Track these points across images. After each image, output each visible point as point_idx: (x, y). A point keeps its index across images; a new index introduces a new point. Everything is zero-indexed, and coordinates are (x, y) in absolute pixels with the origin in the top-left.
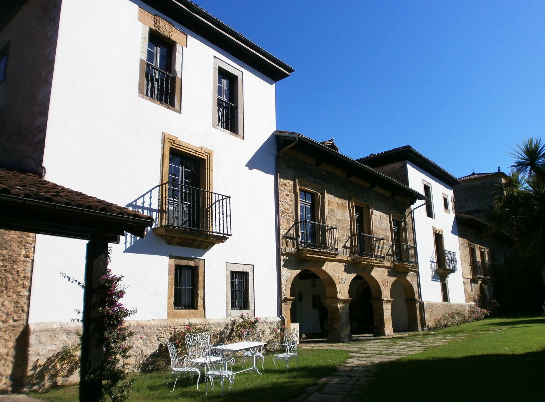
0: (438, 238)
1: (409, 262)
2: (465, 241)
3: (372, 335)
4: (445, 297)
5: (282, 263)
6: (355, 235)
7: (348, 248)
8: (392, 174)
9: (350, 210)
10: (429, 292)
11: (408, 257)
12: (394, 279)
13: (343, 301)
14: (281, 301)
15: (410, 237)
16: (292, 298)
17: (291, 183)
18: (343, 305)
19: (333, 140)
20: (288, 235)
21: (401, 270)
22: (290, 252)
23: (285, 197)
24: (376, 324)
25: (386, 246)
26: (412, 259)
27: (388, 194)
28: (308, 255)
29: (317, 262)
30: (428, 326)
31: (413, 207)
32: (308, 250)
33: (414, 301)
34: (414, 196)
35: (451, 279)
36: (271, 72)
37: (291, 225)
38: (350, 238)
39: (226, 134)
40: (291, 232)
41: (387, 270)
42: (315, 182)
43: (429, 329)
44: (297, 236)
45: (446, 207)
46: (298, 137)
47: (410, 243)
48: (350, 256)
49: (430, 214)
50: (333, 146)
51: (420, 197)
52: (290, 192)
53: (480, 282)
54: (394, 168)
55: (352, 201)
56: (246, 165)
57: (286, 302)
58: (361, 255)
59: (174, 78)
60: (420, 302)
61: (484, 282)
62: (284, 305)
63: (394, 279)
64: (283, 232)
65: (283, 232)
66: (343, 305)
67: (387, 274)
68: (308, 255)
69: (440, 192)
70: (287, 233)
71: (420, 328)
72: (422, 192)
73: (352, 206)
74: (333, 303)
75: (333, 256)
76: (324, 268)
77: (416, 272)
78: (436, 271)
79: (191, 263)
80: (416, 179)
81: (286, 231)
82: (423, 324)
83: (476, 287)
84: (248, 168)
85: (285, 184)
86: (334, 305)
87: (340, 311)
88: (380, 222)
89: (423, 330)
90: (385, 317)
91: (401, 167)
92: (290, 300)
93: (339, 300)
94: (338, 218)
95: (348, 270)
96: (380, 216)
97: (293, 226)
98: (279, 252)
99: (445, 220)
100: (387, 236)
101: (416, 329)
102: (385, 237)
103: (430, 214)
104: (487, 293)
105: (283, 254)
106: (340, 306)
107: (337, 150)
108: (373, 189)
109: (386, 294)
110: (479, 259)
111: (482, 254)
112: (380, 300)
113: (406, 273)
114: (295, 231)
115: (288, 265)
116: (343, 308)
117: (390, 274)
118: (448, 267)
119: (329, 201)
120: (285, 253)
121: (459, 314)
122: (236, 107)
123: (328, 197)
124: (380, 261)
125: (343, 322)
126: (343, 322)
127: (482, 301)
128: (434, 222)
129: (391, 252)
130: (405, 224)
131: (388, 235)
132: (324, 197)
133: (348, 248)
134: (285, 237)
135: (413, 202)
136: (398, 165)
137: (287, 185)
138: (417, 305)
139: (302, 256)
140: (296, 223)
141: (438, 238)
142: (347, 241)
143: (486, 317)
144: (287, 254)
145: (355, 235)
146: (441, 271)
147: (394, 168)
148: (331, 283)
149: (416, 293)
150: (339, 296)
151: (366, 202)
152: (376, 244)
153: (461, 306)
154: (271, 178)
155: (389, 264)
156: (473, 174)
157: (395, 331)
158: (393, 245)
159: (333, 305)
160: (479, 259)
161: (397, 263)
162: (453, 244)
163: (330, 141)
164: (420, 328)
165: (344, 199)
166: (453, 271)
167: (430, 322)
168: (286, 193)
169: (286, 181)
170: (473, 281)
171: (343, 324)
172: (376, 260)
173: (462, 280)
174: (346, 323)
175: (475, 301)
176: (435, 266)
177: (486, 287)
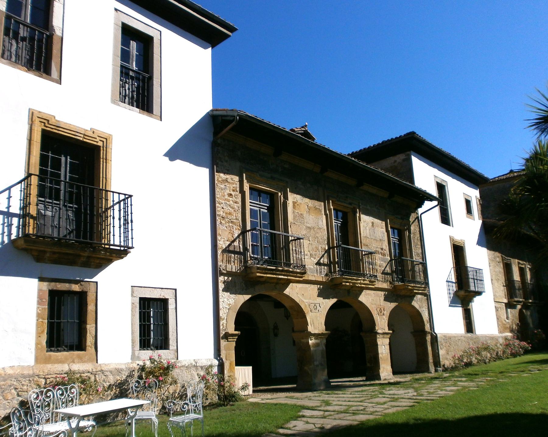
0: (458, 251)
1: (415, 282)
2: (497, 254)
3: (364, 378)
4: (469, 327)
5: (221, 286)
6: (333, 248)
7: (324, 265)
8: (392, 170)
9: (326, 214)
10: (446, 321)
11: (414, 276)
12: (393, 305)
13: (317, 336)
14: (219, 337)
15: (416, 250)
16: (237, 332)
17: (236, 178)
18: (317, 341)
19: (306, 126)
20: (231, 248)
21: (403, 293)
22: (234, 270)
23: (226, 197)
24: (368, 365)
25: (381, 262)
26: (420, 278)
27: (383, 194)
28: (258, 274)
29: (277, 283)
30: (444, 366)
31: (420, 211)
32: (258, 268)
33: (424, 333)
34: (422, 197)
35: (477, 304)
36: (204, 31)
37: (236, 235)
38: (327, 251)
39: (134, 115)
40: (236, 244)
41: (383, 293)
42: (273, 178)
43: (445, 370)
44: (245, 249)
45: (469, 210)
46: (238, 115)
47: (417, 258)
48: (326, 275)
49: (445, 219)
50: (306, 134)
51: (430, 198)
52: (234, 191)
53: (519, 307)
54: (395, 161)
55: (329, 203)
56: (166, 155)
57: (227, 339)
58: (343, 273)
59: (50, 38)
60: (432, 335)
61: (525, 306)
62: (223, 343)
63: (393, 305)
64: (222, 244)
65: (222, 244)
66: (317, 341)
67: (382, 298)
68: (258, 274)
69: (459, 191)
70: (229, 245)
71: (432, 368)
72: (433, 191)
73: (330, 210)
74: (303, 339)
75: (300, 275)
76: (288, 291)
77: (425, 295)
78: (456, 294)
79: (76, 288)
80: (425, 175)
81: (228, 243)
82: (437, 363)
83: (514, 313)
84: (167, 158)
85: (226, 181)
86: (304, 341)
87: (312, 349)
88: (372, 231)
89: (436, 371)
90: (380, 356)
91: (404, 160)
92: (233, 335)
93: (310, 334)
94: (308, 225)
95: (323, 294)
96: (373, 223)
97: (238, 236)
98: (216, 272)
99: (468, 228)
100: (382, 249)
101: (427, 370)
102: (380, 251)
103: (445, 219)
104: (530, 321)
105: (222, 274)
106: (312, 342)
107: (314, 139)
108: (361, 188)
109: (382, 324)
110: (516, 277)
111: (522, 271)
112: (373, 332)
113: (412, 296)
114: (241, 243)
115: (229, 288)
116: (316, 345)
117: (387, 299)
118: (472, 288)
119: (294, 203)
120: (225, 272)
121: (487, 349)
122: (151, 78)
123: (292, 198)
124: (370, 281)
125: (316, 363)
126: (316, 363)
127: (522, 331)
128: (451, 230)
129: (388, 270)
130: (410, 232)
131: (384, 247)
132: (286, 198)
133: (324, 265)
134: (226, 251)
135: (420, 205)
136: (400, 157)
137: (229, 183)
138: (428, 338)
139: (252, 276)
140: (244, 232)
141: (458, 251)
142: (323, 256)
143: (526, 352)
144: (229, 274)
145: (333, 248)
146: (462, 293)
147: (395, 161)
148: (300, 313)
149: (426, 322)
150: (310, 329)
151: (350, 204)
152: (366, 259)
153: (492, 338)
154: (205, 172)
155: (385, 286)
156: (511, 171)
157: (394, 373)
158: (391, 260)
159: (303, 340)
160: (516, 277)
161: (396, 283)
162: (479, 258)
163: (303, 127)
164: (432, 368)
165: (318, 199)
166: (479, 293)
167: (446, 359)
168: (228, 191)
169: (228, 177)
170: (509, 305)
171: (317, 366)
172: (364, 280)
173: (493, 305)
174: (321, 365)
175: (512, 331)
176: (454, 288)
177: (527, 313)
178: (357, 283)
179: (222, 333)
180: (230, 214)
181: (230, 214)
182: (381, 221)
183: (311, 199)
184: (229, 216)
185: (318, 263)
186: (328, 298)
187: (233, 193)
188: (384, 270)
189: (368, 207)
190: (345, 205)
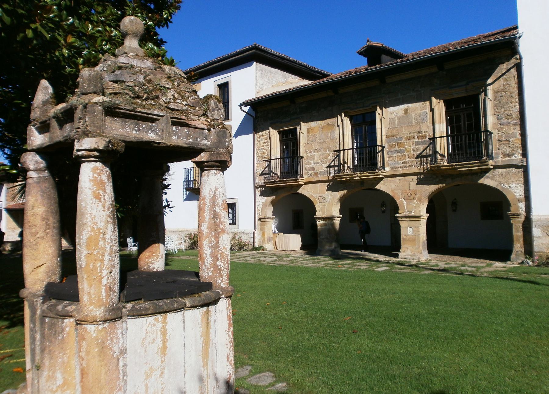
18: (326, 222)
20: (265, 172)
41: (416, 177)
66: (326, 222)
85: (262, 135)
87: (319, 227)
94: (320, 141)
98: (256, 187)
105: (257, 188)
106: (319, 223)
115: (263, 194)
117: (420, 182)
134: (262, 174)
144: (260, 187)
168: (263, 141)
169: (263, 133)
171: (323, 239)
178: (356, 177)
179: (257, 218)
180: (264, 153)
181: (264, 153)
182: (421, 103)
183: (324, 120)
184: (263, 155)
185: (329, 166)
186: (337, 190)
187: (266, 141)
188: (421, 153)
189: (400, 96)
190: (365, 108)
